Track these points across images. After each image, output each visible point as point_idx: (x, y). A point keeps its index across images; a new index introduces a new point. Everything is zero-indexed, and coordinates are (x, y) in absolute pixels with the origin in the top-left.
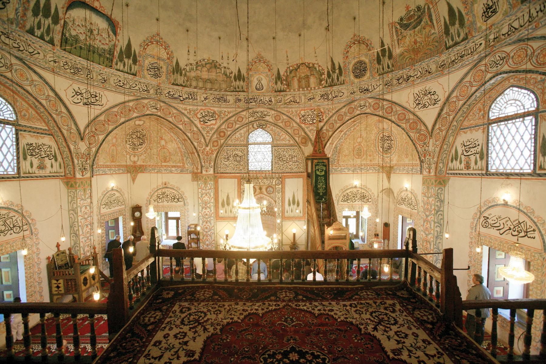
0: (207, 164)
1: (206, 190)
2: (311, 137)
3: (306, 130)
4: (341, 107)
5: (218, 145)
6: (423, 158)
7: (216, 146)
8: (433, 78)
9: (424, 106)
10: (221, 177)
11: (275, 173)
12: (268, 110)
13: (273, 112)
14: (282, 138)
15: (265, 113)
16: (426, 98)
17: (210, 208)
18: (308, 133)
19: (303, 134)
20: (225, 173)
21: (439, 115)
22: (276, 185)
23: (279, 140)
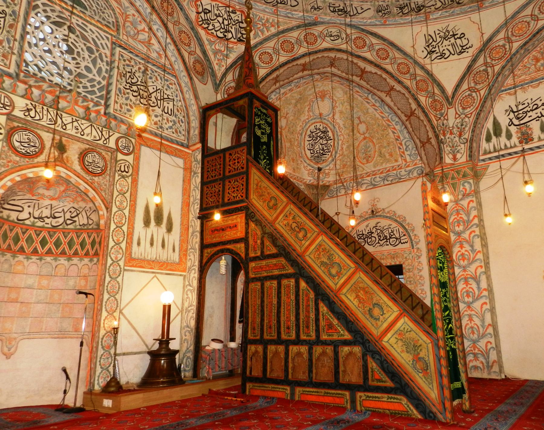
2: (216, 67)
4: (290, 26)
6: (443, 137)
8: (462, 13)
9: (442, 56)
11: (115, 118)
16: (446, 43)
18: (212, 57)
19: (198, 51)
21: (469, 68)
22: (118, 150)
23: (132, 38)
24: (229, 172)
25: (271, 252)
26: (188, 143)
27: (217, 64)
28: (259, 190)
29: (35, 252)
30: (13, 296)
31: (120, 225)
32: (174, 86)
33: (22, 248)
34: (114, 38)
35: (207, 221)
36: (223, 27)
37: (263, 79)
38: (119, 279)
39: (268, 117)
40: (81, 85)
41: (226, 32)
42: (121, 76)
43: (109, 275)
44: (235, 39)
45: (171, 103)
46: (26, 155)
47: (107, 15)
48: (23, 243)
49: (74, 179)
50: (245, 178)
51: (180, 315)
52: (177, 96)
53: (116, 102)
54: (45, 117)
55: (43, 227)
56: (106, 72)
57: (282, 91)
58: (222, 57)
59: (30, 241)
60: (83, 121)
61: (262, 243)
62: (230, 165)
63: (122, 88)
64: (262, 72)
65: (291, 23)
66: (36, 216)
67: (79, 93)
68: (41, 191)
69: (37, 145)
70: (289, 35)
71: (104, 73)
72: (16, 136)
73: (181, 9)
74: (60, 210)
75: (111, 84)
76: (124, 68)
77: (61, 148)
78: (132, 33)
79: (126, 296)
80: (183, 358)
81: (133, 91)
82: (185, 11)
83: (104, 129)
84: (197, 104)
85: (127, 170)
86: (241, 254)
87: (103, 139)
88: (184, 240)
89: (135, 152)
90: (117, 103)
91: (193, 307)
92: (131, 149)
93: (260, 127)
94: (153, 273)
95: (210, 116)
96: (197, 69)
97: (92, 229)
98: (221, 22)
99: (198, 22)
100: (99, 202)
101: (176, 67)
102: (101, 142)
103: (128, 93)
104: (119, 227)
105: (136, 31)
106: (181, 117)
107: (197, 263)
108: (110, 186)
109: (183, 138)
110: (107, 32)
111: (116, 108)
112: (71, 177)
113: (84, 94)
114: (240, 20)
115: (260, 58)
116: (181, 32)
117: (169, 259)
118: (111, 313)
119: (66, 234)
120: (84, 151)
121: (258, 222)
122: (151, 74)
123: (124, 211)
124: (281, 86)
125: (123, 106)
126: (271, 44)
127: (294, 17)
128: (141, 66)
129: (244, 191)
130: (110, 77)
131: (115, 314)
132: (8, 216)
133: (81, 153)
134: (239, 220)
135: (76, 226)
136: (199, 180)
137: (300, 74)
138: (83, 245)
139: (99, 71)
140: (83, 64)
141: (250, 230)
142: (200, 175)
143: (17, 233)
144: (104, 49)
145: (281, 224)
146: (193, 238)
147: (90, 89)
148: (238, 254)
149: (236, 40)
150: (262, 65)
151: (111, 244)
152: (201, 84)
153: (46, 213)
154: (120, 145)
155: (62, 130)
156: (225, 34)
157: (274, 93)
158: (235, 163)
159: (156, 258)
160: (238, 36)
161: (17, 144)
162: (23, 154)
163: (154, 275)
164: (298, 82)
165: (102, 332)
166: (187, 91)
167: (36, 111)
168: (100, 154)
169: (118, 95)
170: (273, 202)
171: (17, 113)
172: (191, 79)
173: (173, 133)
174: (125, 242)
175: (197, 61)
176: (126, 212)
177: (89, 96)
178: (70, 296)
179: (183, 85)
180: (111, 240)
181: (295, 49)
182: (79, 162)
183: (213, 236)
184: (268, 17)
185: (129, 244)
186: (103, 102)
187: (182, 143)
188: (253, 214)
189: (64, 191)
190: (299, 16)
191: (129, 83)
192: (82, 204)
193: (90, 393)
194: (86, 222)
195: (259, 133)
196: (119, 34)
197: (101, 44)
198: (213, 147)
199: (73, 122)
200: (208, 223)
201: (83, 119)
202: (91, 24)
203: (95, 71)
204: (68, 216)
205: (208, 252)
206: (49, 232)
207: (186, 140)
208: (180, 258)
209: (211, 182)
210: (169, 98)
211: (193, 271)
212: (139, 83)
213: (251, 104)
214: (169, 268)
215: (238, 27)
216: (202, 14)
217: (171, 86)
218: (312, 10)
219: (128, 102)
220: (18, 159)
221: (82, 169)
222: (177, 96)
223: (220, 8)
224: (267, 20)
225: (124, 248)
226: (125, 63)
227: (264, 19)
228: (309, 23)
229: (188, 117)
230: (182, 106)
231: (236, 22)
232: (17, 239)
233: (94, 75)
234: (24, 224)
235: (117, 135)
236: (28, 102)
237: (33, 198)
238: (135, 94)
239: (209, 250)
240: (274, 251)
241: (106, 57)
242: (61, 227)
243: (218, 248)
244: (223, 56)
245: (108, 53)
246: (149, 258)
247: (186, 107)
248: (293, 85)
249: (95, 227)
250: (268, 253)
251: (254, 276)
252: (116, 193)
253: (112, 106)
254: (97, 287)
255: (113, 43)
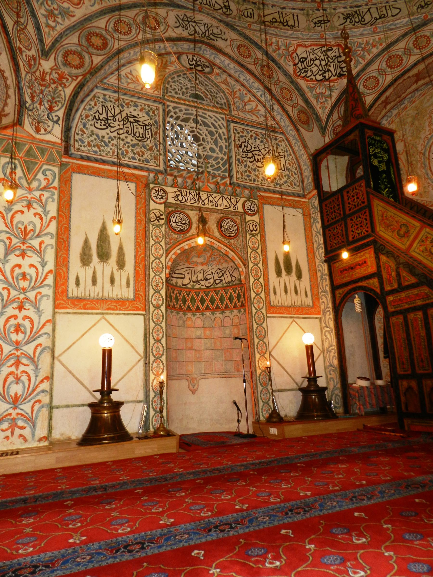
0: (43, 110)
1: (30, 190)
2: (320, 111)
3: (309, 95)
4: (394, 38)
5: (81, 66)
7: (77, 67)
10: (81, 170)
11: (239, 186)
12: (222, 27)
13: (234, 35)
14: (248, 107)
15: (215, 31)
17: (39, 252)
19: (301, 102)
20: (96, 161)
22: (245, 212)
23: (243, 111)
24: (350, 210)
25: (410, 283)
26: (304, 192)
27: (320, 108)
28: (385, 221)
29: (198, 309)
30: (189, 345)
31: (257, 278)
32: (283, 143)
33: (189, 307)
34: (227, 117)
35: (333, 264)
36: (321, 69)
37: (371, 106)
38: (264, 325)
39: (384, 144)
40: (209, 165)
41: (325, 72)
42: (238, 148)
43: (256, 322)
44: (335, 76)
45: (283, 159)
46: (181, 232)
47: (219, 99)
48: (189, 303)
49: (216, 244)
50: (367, 212)
51: (322, 355)
52: (287, 151)
53: (237, 172)
54: (189, 198)
55: (200, 289)
56: (226, 148)
57: (395, 112)
58: (324, 99)
59: (193, 301)
60: (216, 195)
61: (398, 275)
62: (349, 203)
63: (240, 157)
64: (369, 100)
65: (395, 34)
66: (194, 280)
67: (209, 172)
68: (195, 259)
69: (187, 222)
70: (394, 49)
71: (225, 150)
72: (172, 218)
73: (279, 68)
74: (210, 273)
75: (231, 157)
76: (239, 140)
77: (203, 220)
78: (241, 106)
79: (272, 340)
80: (332, 396)
81: (249, 158)
82: (282, 68)
83: (232, 197)
84: (307, 152)
85: (255, 229)
86: (375, 289)
87: (233, 206)
88: (314, 284)
89: (259, 212)
90: (238, 172)
91: (333, 347)
92: (256, 210)
93: (375, 156)
94: (291, 317)
95: (321, 161)
96: (302, 119)
97: (236, 284)
98: (318, 65)
99: (296, 73)
100: (237, 260)
101: (282, 124)
102: (231, 209)
103: (245, 161)
104: (257, 280)
105: (244, 104)
106: (293, 170)
107: (330, 305)
108: (244, 245)
109: (298, 189)
110: (221, 113)
111: (238, 177)
112: (214, 243)
113: (212, 172)
114: (337, 54)
115: (364, 86)
116: (282, 89)
117: (303, 304)
118: (263, 355)
119: (217, 292)
120: (220, 220)
121: (389, 254)
122: (262, 138)
123: (259, 265)
124: (392, 108)
125: (243, 174)
126: (375, 66)
127: (398, 26)
128: (252, 133)
129: (369, 225)
130: (230, 151)
131: (266, 355)
132: (176, 283)
133: (218, 222)
134: (367, 255)
135: (223, 284)
136: (319, 225)
137: (414, 87)
138: (231, 299)
139: (221, 149)
140: (208, 147)
141: (381, 264)
142: (319, 220)
143: (184, 296)
144: (221, 128)
145: (418, 251)
146: (323, 282)
147: (216, 166)
148: (372, 290)
149: (336, 77)
150: (368, 91)
151: (253, 295)
152: (308, 133)
153: (201, 276)
154: (246, 208)
155: (202, 206)
156: (324, 75)
157: (385, 118)
158: (354, 200)
159: (292, 304)
160: (338, 72)
161: (174, 225)
162: (179, 231)
163: (292, 320)
164: (412, 97)
165: (258, 372)
166: (295, 143)
167: (182, 195)
168: (231, 219)
169: (238, 165)
170: (403, 230)
171: (171, 200)
172: (298, 130)
173: (289, 186)
174: (263, 292)
175: (301, 112)
176: (260, 265)
177: (216, 172)
178: (227, 343)
179: (291, 139)
180: (252, 291)
181: (404, 61)
182: (218, 229)
183: (342, 276)
184: (368, 39)
185: (267, 294)
186: (227, 174)
187: (298, 194)
188: (382, 246)
189: (210, 256)
190: (404, 23)
191: (245, 152)
192: (225, 265)
193: (257, 422)
194: (230, 280)
195: (375, 162)
196: (230, 111)
197: (219, 125)
198: (329, 190)
199: (208, 197)
200: (335, 264)
201: (215, 192)
202: (209, 111)
203: (217, 150)
204: (216, 277)
205: (340, 292)
206: (205, 292)
207: (301, 190)
208: (313, 302)
209: (331, 224)
210: (280, 155)
211: (328, 313)
212: (253, 149)
213: (362, 135)
214: (304, 312)
215: (336, 62)
216: (299, 65)
217: (280, 144)
218: (419, 10)
219: (247, 168)
220: (176, 236)
221: (221, 235)
222: (287, 151)
223: (315, 52)
224: (367, 43)
225: (264, 298)
226: (239, 135)
227: (362, 44)
228: (418, 25)
229: (300, 168)
230: (292, 159)
231: (334, 58)
232: (184, 301)
233: (217, 154)
234: (187, 288)
235: (243, 200)
236: (176, 189)
237: (190, 266)
238: (251, 160)
239: (341, 291)
240: (412, 280)
241: (224, 135)
242: (212, 287)
243: (350, 287)
244: (325, 98)
245: (225, 131)
246: (286, 305)
247: (297, 159)
248: (406, 102)
249: (238, 282)
250: (406, 283)
251: (393, 310)
252: (249, 251)
253: (235, 176)
254: (248, 333)
255: (228, 121)
